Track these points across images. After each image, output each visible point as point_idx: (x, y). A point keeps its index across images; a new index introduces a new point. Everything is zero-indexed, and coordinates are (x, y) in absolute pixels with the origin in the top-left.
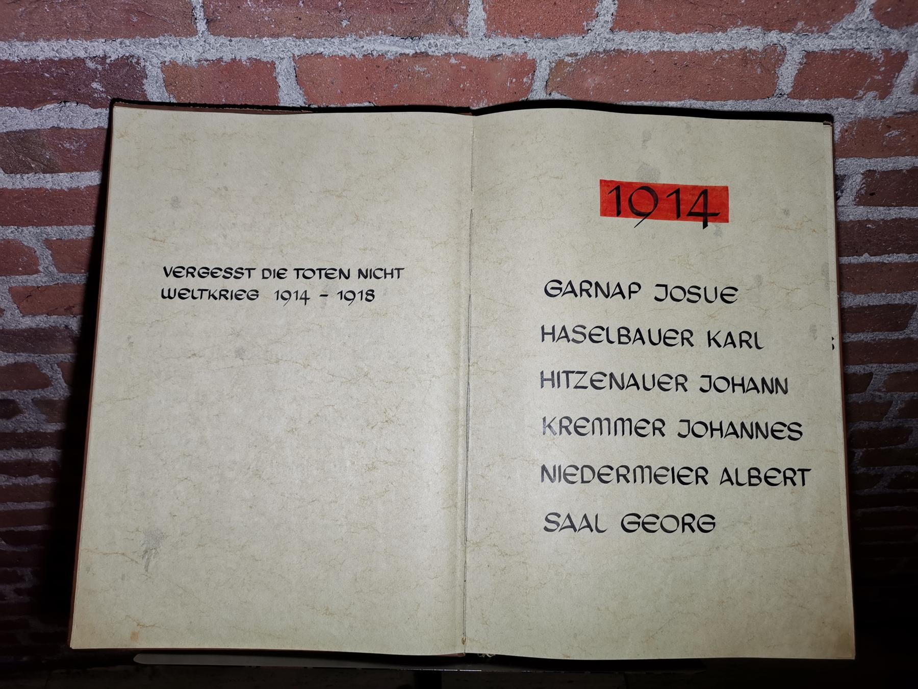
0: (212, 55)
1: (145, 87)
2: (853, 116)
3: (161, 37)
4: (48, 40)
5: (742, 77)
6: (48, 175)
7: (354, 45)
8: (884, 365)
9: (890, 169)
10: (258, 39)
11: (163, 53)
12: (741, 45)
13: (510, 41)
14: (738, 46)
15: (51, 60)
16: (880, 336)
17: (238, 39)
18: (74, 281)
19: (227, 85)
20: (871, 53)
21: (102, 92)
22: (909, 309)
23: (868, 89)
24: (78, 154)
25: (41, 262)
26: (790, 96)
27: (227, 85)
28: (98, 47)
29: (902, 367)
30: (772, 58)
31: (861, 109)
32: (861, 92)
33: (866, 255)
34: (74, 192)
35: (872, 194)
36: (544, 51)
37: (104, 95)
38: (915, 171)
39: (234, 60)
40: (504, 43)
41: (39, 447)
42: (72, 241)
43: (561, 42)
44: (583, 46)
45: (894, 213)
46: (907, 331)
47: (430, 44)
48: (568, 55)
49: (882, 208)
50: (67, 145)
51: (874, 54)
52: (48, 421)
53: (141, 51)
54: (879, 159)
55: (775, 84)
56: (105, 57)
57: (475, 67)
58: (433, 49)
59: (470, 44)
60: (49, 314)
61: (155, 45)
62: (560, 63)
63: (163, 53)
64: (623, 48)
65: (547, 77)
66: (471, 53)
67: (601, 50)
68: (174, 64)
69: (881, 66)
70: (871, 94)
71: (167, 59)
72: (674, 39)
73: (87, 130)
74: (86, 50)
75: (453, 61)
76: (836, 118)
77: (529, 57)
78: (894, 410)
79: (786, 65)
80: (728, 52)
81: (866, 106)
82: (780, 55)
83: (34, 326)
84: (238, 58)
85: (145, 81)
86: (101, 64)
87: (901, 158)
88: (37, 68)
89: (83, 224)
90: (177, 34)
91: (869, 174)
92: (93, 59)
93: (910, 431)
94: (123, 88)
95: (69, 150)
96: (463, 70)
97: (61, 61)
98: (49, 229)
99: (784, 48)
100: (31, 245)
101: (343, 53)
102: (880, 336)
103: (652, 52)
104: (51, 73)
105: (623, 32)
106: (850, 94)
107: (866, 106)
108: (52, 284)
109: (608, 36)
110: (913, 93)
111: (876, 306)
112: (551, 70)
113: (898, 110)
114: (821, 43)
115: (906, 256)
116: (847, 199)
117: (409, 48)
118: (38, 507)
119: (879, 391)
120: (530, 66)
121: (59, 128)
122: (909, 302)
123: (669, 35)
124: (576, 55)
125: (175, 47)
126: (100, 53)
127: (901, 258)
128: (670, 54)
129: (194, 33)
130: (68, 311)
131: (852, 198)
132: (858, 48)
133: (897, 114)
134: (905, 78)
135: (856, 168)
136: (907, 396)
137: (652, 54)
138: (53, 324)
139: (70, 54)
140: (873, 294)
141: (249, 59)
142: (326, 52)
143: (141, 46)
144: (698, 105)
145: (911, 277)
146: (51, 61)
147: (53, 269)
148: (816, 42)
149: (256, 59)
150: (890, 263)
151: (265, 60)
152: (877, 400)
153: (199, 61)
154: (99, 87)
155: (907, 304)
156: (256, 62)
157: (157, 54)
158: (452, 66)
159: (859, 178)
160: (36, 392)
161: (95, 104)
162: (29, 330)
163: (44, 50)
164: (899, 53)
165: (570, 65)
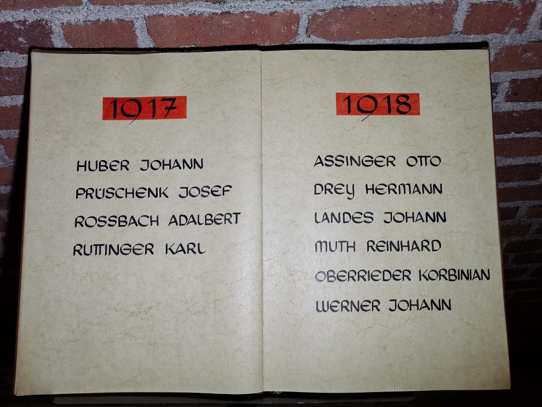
0: (92, 18)
1: (52, 40)
2: (502, 45)
3: (60, 7)
5: (430, 21)
7: (183, 8)
8: (526, 201)
10: (121, 6)
11: (62, 17)
16: (524, 183)
17: (109, 7)
19: (104, 36)
23: (512, 27)
24: (15, 84)
26: (462, 33)
27: (104, 36)
28: (20, 15)
31: (507, 40)
32: (507, 29)
33: (513, 133)
35: (516, 94)
37: (27, 46)
38: (541, 80)
44: (329, 4)
45: (530, 106)
46: (540, 180)
48: (319, 11)
49: (522, 103)
50: (7, 78)
51: (515, 3)
53: (47, 16)
55: (452, 25)
56: (25, 21)
58: (233, 9)
61: (56, 12)
62: (315, 16)
63: (62, 17)
65: (307, 25)
66: (257, 11)
67: (340, 6)
68: (69, 24)
70: (514, 30)
71: (65, 21)
73: (18, 68)
74: (12, 16)
75: (246, 16)
76: (491, 45)
77: (295, 13)
78: (533, 228)
79: (459, 12)
80: (421, 6)
82: (454, 6)
85: (52, 36)
86: (23, 26)
87: (533, 71)
90: (69, 5)
91: (514, 81)
94: (38, 41)
95: (8, 81)
102: (524, 183)
103: (373, 7)
106: (500, 31)
110: (540, 28)
111: (520, 165)
112: (309, 21)
113: (531, 40)
115: (538, 133)
116: (500, 98)
117: (218, 9)
119: (523, 217)
120: (296, 19)
124: (324, 10)
125: (69, 13)
126: (22, 18)
127: (536, 134)
129: (81, 3)
134: (534, 19)
135: (505, 77)
139: (3, 20)
140: (518, 158)
142: (165, 13)
143: (47, 13)
144: (403, 41)
145: (541, 147)
147: (5, 157)
150: (528, 138)
151: (127, 20)
152: (522, 223)
153: (85, 22)
154: (23, 40)
157: (58, 18)
158: (246, 20)
159: (507, 85)
165: (321, 17)
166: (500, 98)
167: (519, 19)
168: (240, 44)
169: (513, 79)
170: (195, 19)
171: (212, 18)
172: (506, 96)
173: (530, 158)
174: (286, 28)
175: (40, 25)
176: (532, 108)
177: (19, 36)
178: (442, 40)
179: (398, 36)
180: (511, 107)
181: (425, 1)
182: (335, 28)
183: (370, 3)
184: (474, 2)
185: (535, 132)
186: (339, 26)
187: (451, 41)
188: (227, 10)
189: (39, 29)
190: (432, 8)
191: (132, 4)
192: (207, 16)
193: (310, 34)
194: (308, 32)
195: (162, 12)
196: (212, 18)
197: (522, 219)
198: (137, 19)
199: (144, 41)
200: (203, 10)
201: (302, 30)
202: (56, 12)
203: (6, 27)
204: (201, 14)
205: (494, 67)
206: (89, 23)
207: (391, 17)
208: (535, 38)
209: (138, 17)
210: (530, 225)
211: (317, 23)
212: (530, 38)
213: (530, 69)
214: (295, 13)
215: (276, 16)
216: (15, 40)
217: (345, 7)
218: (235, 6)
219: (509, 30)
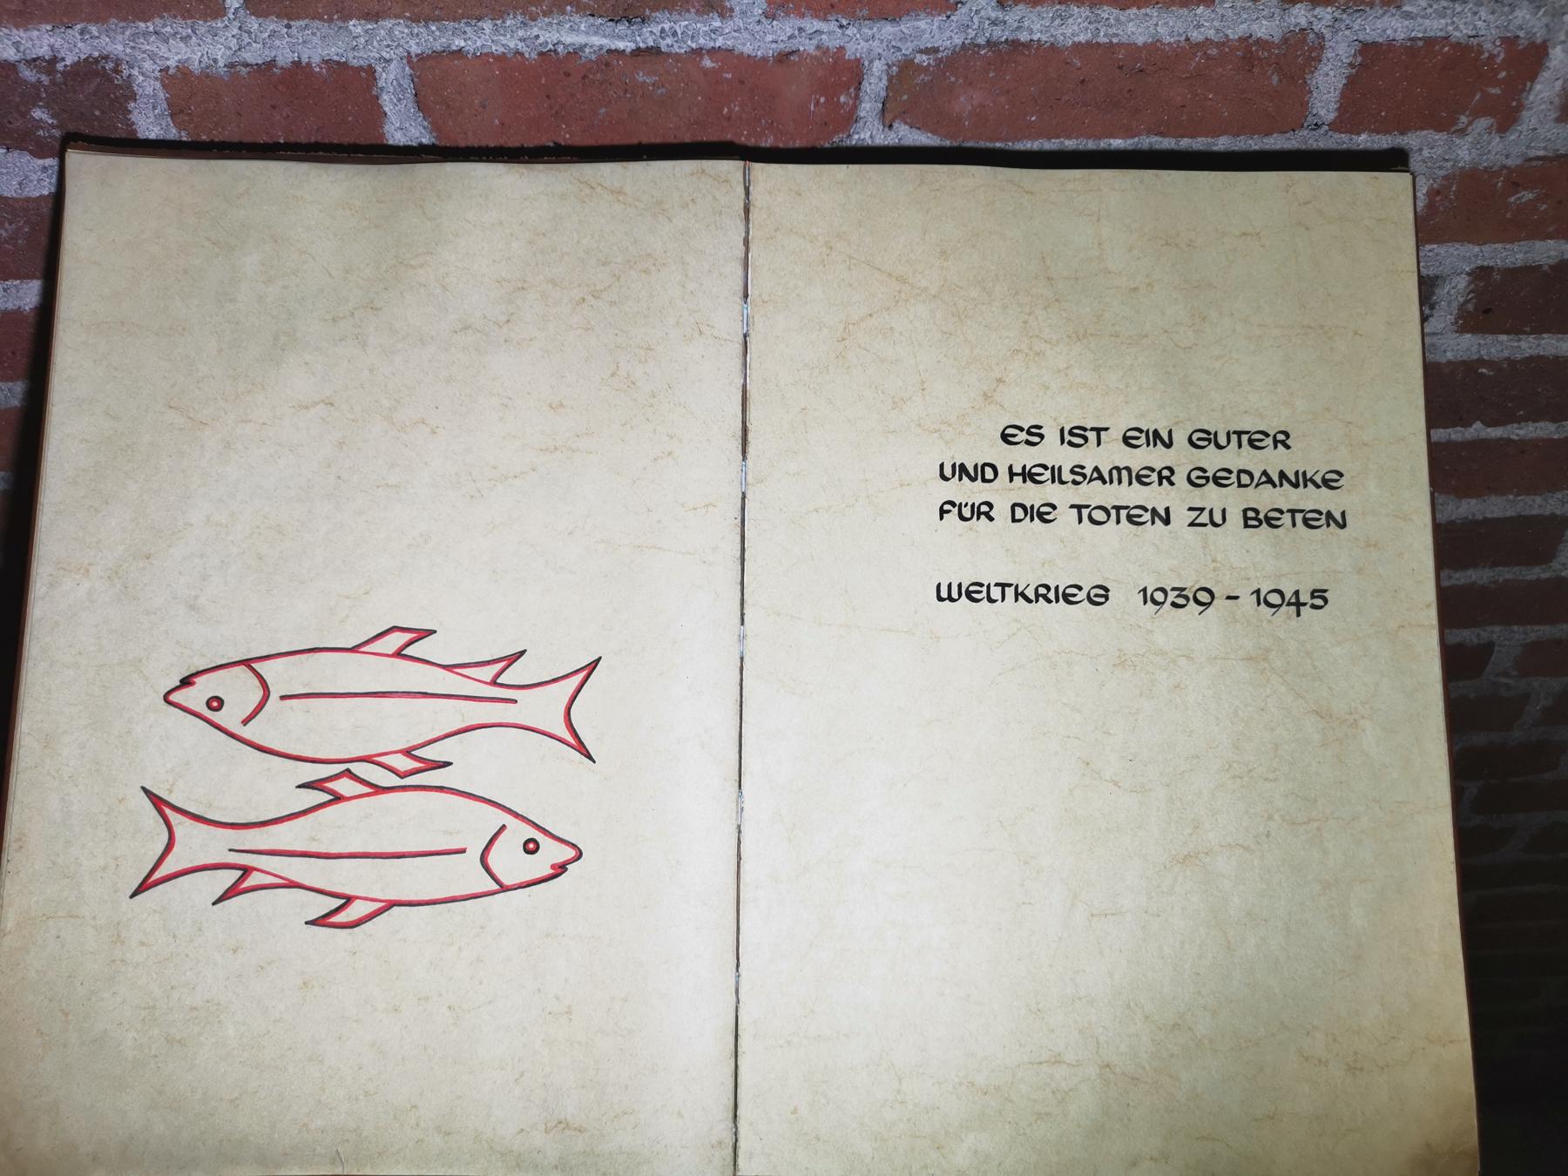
0: (254, 55)
1: (134, 117)
2: (1449, 164)
3: (158, 21)
7: (521, 33)
8: (1515, 628)
9: (1519, 264)
10: (340, 24)
11: (163, 51)
12: (1241, 30)
13: (812, 25)
14: (1236, 32)
16: (1507, 574)
17: (303, 23)
23: (1478, 113)
26: (1335, 126)
28: (40, 41)
30: (1300, 53)
32: (1464, 119)
33: (1478, 425)
35: (1486, 311)
36: (876, 43)
38: (1565, 269)
39: (297, 64)
40: (800, 29)
43: (906, 26)
44: (948, 34)
45: (1528, 346)
46: (1555, 565)
47: (663, 31)
48: (921, 52)
49: (1503, 338)
51: (1488, 46)
53: (120, 48)
54: (1499, 246)
55: (1305, 105)
56: (54, 60)
57: (749, 76)
58: (669, 41)
61: (146, 34)
62: (907, 66)
63: (163, 50)
64: (1024, 37)
65: (883, 94)
66: (739, 48)
67: (981, 41)
68: (183, 71)
70: (1483, 123)
71: (172, 63)
72: (1117, 19)
73: (28, 200)
74: (17, 45)
75: (707, 63)
76: (1415, 162)
77: (849, 55)
79: (1324, 68)
80: (1220, 45)
81: (1471, 146)
82: (1312, 49)
84: (305, 60)
85: (132, 105)
87: (1538, 244)
90: (187, 14)
92: (33, 62)
94: (93, 120)
96: (728, 81)
99: (1320, 36)
102: (1507, 574)
103: (1077, 45)
105: (1021, 6)
106: (1442, 120)
107: (1471, 146)
109: (993, 15)
110: (1558, 120)
112: (890, 79)
113: (1532, 153)
114: (1389, 27)
115: (1552, 427)
119: (1506, 674)
120: (853, 73)
123: (1106, 12)
124: (936, 50)
125: (185, 39)
126: (44, 51)
127: (1542, 430)
129: (218, 11)
131: (1450, 318)
133: (1530, 160)
134: (1543, 92)
136: (1556, 684)
140: (1493, 498)
143: (120, 37)
148: (1379, 24)
149: (338, 63)
151: (355, 63)
153: (231, 65)
154: (45, 117)
155: (1553, 516)
156: (338, 68)
158: (706, 72)
159: (1462, 282)
161: (40, 151)
164: (1533, 44)
166: (1443, 319)
167: (1495, 91)
168: (687, 138)
169: (1482, 268)
171: (607, 65)
172: (1459, 317)
173: (1528, 499)
174: (822, 100)
175: (96, 73)
179: (1150, 132)
180: (1474, 349)
181: (1229, 32)
182: (965, 103)
183: (1069, 32)
184: (1369, 39)
185: (1541, 424)
186: (978, 96)
189: (93, 86)
191: (373, 16)
192: (593, 57)
193: (893, 120)
194: (887, 116)
195: (459, 43)
196: (607, 65)
197: (1503, 680)
198: (388, 61)
199: (403, 124)
200: (579, 39)
201: (868, 108)
202: (146, 34)
204: (575, 53)
205: (1427, 229)
206: (244, 71)
207: (1129, 77)
208: (1545, 148)
209: (387, 56)
211: (913, 88)
212: (1528, 147)
213: (1528, 238)
214: (849, 55)
215: (795, 63)
216: (23, 115)
217: (996, 44)
219: (1470, 123)
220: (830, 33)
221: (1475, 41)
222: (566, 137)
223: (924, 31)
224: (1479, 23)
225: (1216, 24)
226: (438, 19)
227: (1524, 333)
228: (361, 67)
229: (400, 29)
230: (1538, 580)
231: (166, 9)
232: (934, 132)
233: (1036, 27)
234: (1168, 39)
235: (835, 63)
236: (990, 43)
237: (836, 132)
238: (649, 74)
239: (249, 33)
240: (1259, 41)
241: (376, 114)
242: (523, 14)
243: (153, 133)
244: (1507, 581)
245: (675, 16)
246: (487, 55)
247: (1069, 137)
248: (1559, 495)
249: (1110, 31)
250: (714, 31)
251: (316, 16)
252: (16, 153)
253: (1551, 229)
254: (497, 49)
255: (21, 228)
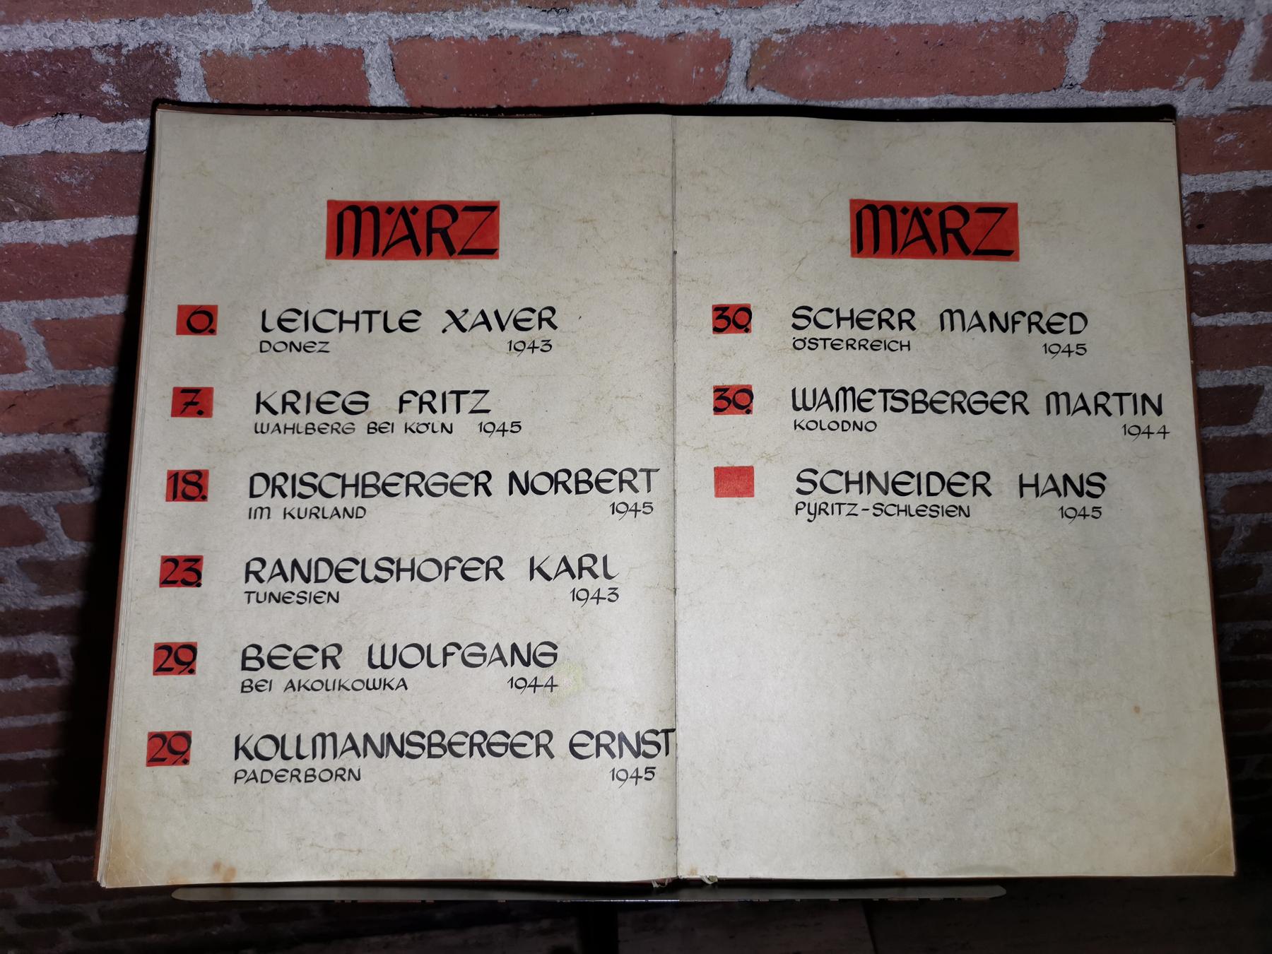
0: (272, 41)
1: (178, 90)
3: (201, 15)
4: (39, 21)
6: (38, 224)
7: (475, 21)
8: (1222, 475)
10: (339, 15)
11: (204, 38)
12: (1016, 13)
13: (695, 12)
15: (43, 51)
18: (77, 381)
20: (1193, 23)
21: (116, 97)
22: (1251, 394)
23: (1191, 75)
24: (82, 191)
25: (29, 353)
26: (1086, 86)
28: (110, 31)
29: (1244, 477)
30: (1058, 31)
32: (1182, 79)
34: (77, 248)
35: (1200, 227)
36: (743, 26)
37: (119, 102)
39: (305, 47)
41: (28, 633)
42: (74, 321)
43: (766, 13)
44: (797, 18)
46: (1252, 424)
47: (583, 18)
48: (777, 32)
49: (1212, 247)
50: (66, 178)
51: (1199, 23)
52: (43, 593)
53: (171, 36)
54: (1209, 176)
55: (1063, 70)
56: (119, 47)
57: (645, 51)
59: (640, 18)
60: (42, 431)
62: (766, 43)
64: (854, 20)
65: (747, 65)
67: (822, 23)
68: (219, 53)
69: (1209, 40)
70: (1197, 81)
72: (924, 6)
73: (94, 155)
74: (92, 34)
75: (616, 43)
77: (722, 35)
80: (999, 24)
82: (1069, 27)
83: (19, 450)
84: (311, 44)
85: (178, 80)
87: (1237, 174)
88: (22, 65)
89: (91, 296)
90: (223, 9)
91: (1197, 196)
93: (1258, 571)
94: (147, 88)
95: (69, 186)
97: (59, 55)
98: (40, 304)
99: (1075, 17)
100: (13, 329)
101: (460, 34)
104: (42, 71)
107: (1190, 99)
108: (45, 386)
109: (831, 4)
110: (1252, 79)
111: (1210, 389)
112: (753, 53)
113: (1233, 105)
117: (553, 26)
118: (28, 724)
121: (54, 153)
122: (1254, 383)
124: (788, 31)
125: (221, 29)
126: (113, 40)
127: (1241, 318)
128: (919, 27)
129: (248, 7)
130: (71, 426)
132: (1176, 15)
133: (1230, 110)
136: (1254, 519)
137: (894, 28)
138: (48, 447)
139: (69, 42)
141: (327, 45)
146: (42, 53)
147: (46, 364)
151: (349, 46)
153: (255, 49)
155: (1250, 386)
156: (337, 51)
157: (194, 42)
158: (614, 50)
160: (23, 550)
162: (13, 457)
163: (33, 36)
164: (1232, 21)
165: (780, 46)
167: (1205, 57)
170: (502, 45)
171: (540, 45)
175: (152, 56)
176: (1235, 258)
177: (103, 81)
178: (1042, 101)
179: (948, 92)
181: (1007, 15)
182: (809, 71)
184: (1111, 19)
187: (1062, 104)
188: (573, 28)
190: (1022, 31)
194: (750, 81)
195: (429, 29)
198: (374, 44)
201: (736, 76)
202: (192, 25)
203: (74, 58)
204: (516, 37)
210: (1230, 530)
211: (770, 60)
214: (722, 35)
216: (94, 89)
217: (832, 26)
218: (592, 20)
219: (1186, 82)
220: (708, 18)
221: (1190, 20)
222: (507, 102)
223: (779, 17)
224: (1193, 6)
225: (998, 8)
226: (413, 12)
227: (1227, 243)
228: (353, 50)
229: (384, 19)
230: (1239, 437)
231: (207, 6)
232: (786, 93)
233: (863, 13)
234: (961, 21)
235: (712, 41)
236: (828, 26)
237: (712, 94)
238: (570, 51)
239: (270, 23)
240: (1029, 22)
241: (365, 85)
242: (478, 6)
243: (195, 100)
244: (1215, 438)
245: (593, 7)
246: (449, 38)
247: (887, 96)
248: (1254, 370)
249: (918, 15)
250: (621, 18)
251: (321, 10)
252: (86, 120)
253: (1247, 162)
254: (457, 34)
255: (86, 178)
